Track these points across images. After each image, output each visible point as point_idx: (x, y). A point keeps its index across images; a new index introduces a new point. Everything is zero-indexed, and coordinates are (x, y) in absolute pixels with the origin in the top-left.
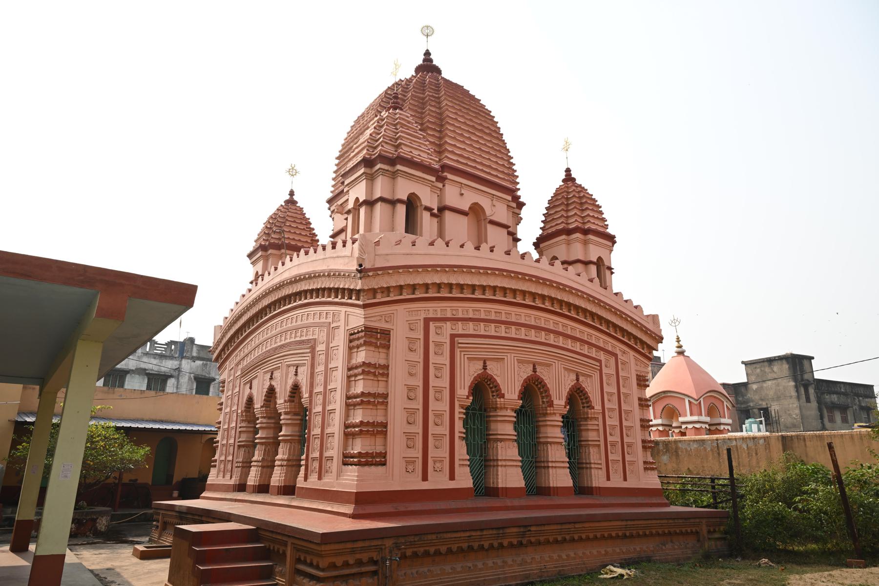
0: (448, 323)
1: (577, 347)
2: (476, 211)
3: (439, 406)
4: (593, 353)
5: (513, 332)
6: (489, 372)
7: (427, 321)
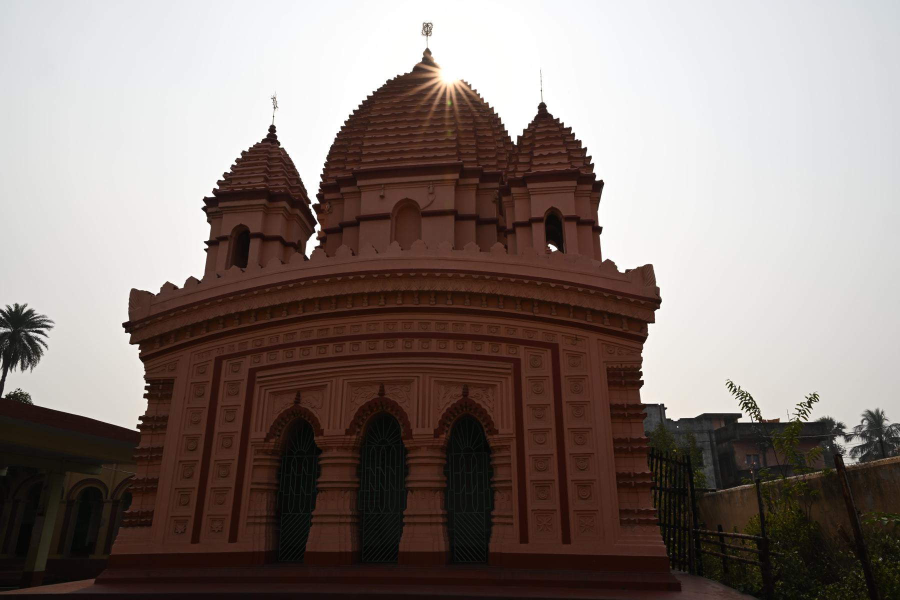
0: (249, 357)
1: (469, 348)
2: (407, 207)
4: (504, 351)
5: (347, 349)
7: (219, 361)
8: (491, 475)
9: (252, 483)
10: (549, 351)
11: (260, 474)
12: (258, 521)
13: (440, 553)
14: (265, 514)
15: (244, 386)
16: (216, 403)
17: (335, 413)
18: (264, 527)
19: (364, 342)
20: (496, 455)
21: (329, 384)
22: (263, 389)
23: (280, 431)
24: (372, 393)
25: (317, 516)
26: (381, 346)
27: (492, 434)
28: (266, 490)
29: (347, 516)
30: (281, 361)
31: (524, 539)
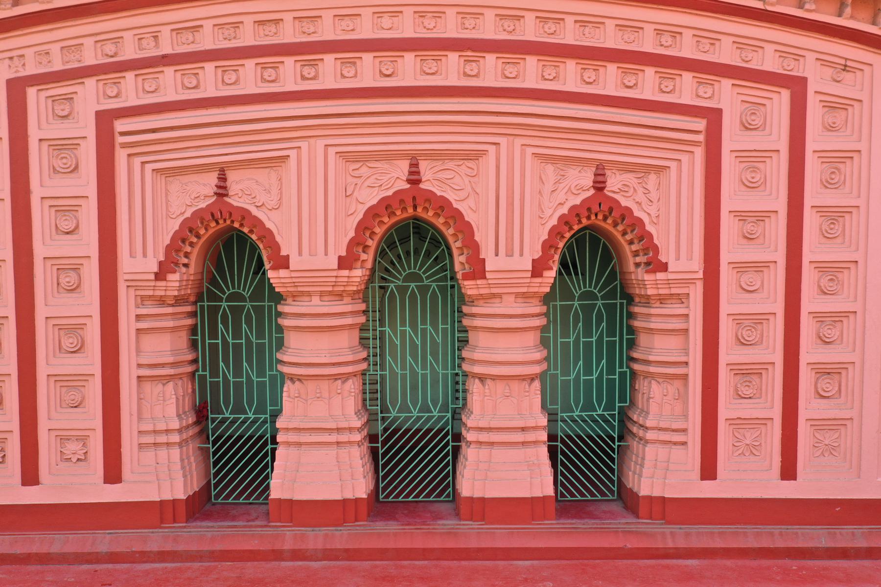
0: (90, 83)
1: (610, 80)
3: (68, 305)
4: (686, 89)
5: (329, 72)
6: (235, 201)
8: (632, 344)
9: (140, 366)
10: (786, 94)
11: (155, 345)
12: (162, 439)
13: (545, 498)
14: (175, 424)
15: (88, 155)
16: (27, 192)
17: (313, 216)
18: (176, 452)
19: (368, 57)
20: (653, 311)
21: (293, 154)
22: (137, 161)
23: (187, 255)
24: (394, 178)
25: (287, 429)
26: (409, 70)
27: (654, 271)
28: (171, 377)
30: (171, 96)
31: (709, 471)
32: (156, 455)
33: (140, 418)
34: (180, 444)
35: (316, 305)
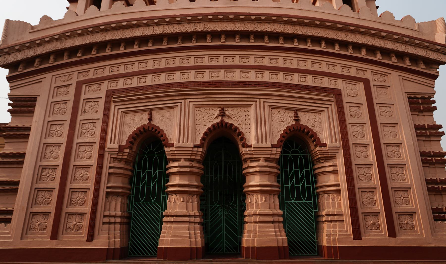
9: (108, 188)
12: (112, 220)
14: (119, 213)
18: (118, 226)
22: (117, 107)
29: (195, 216)
32: (109, 227)
33: (105, 211)
34: (120, 223)
35: (182, 163)
